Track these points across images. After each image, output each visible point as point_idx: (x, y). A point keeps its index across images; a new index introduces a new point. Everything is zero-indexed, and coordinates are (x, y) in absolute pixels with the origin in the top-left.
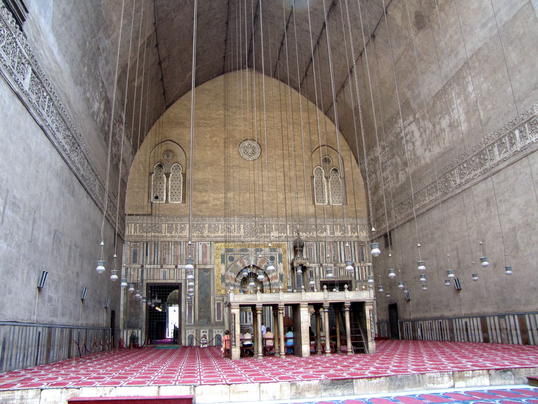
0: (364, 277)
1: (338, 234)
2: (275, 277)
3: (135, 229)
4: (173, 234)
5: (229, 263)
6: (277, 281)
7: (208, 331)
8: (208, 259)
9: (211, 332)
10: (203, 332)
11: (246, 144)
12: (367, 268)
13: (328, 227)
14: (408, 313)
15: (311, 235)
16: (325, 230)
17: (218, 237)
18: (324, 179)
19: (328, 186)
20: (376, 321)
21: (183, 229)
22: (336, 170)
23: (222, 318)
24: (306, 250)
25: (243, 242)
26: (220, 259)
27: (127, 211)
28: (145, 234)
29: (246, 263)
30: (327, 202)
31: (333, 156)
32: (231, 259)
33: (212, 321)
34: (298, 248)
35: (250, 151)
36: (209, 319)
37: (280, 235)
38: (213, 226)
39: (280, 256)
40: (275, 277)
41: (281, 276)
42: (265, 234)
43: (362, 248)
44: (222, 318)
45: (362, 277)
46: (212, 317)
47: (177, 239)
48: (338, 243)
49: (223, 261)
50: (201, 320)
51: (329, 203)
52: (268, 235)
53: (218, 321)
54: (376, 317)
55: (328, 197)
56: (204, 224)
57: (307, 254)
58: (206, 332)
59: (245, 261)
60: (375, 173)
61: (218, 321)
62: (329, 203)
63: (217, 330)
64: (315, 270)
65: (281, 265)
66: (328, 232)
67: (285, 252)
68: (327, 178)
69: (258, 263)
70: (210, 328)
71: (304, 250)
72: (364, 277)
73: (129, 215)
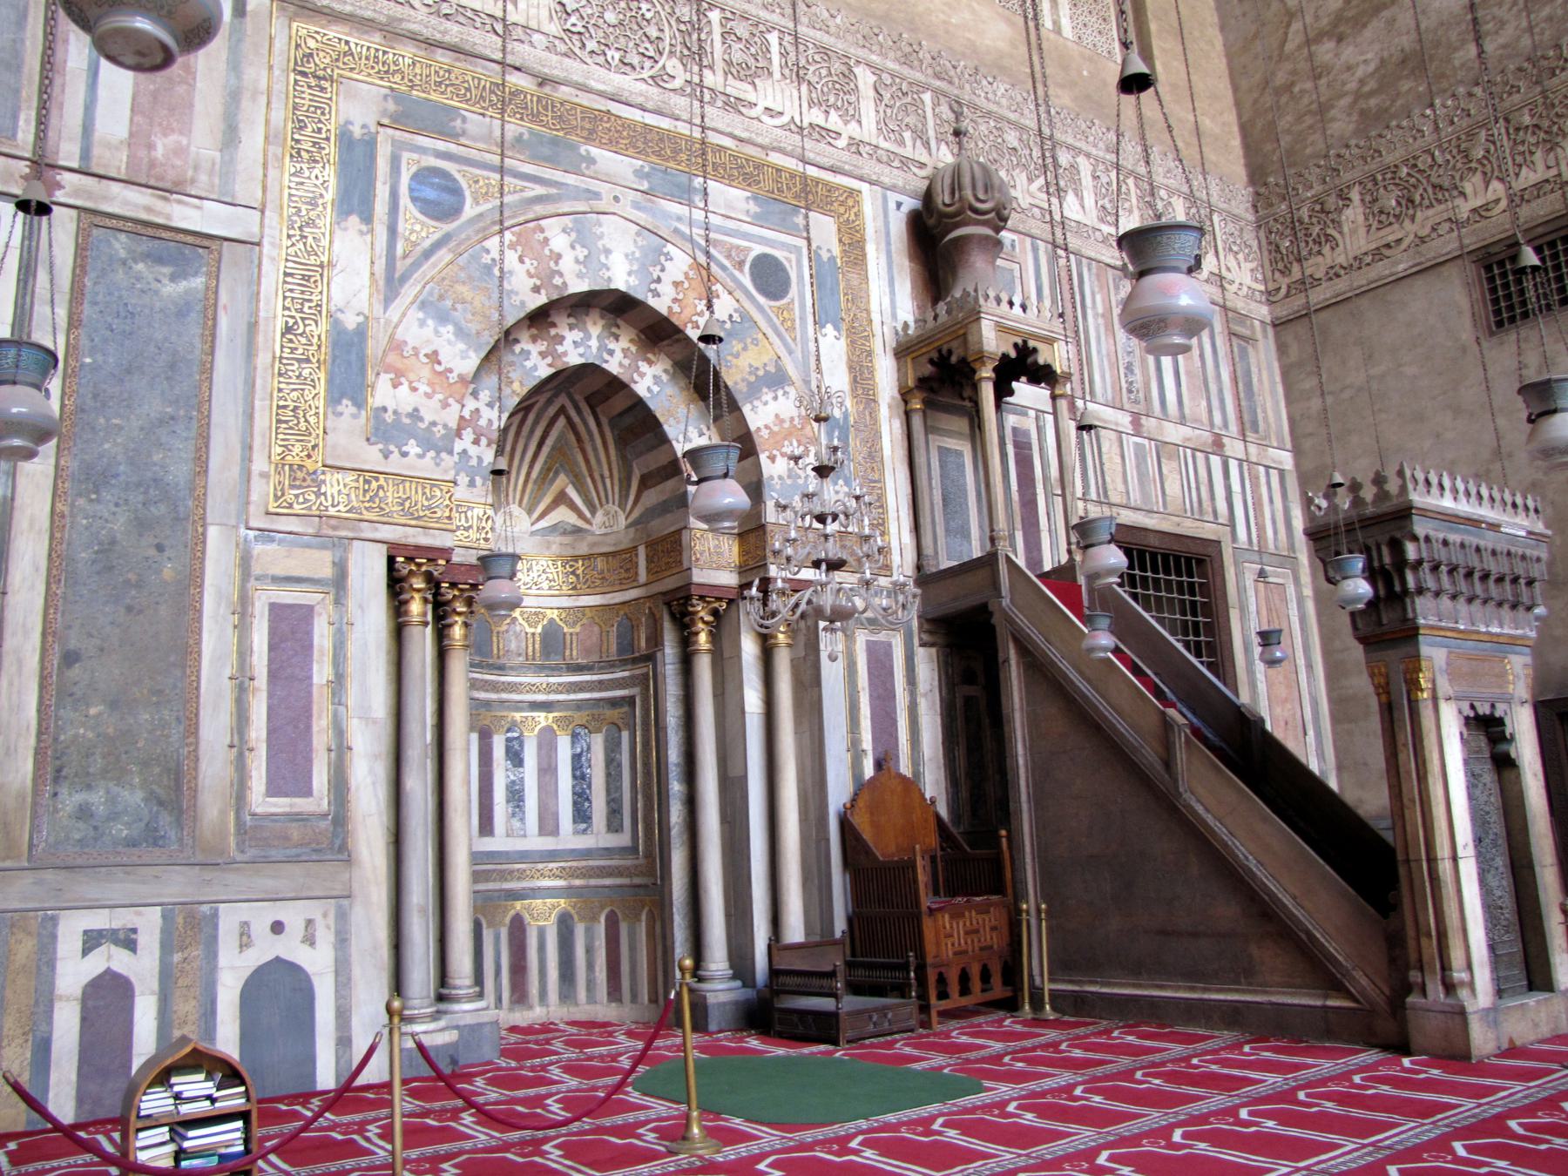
5: (416, 227)
7: (149, 924)
8: (202, 140)
9: (191, 932)
10: (92, 941)
23: (320, 778)
25: (543, 81)
26: (330, 174)
29: (567, 265)
32: (440, 197)
33: (212, 806)
34: (940, 240)
36: (174, 788)
43: (1244, 354)
44: (320, 778)
46: (213, 767)
49: (355, 199)
50: (71, 799)
53: (281, 805)
58: (128, 941)
59: (559, 242)
61: (281, 805)
63: (261, 917)
69: (667, 290)
70: (178, 885)
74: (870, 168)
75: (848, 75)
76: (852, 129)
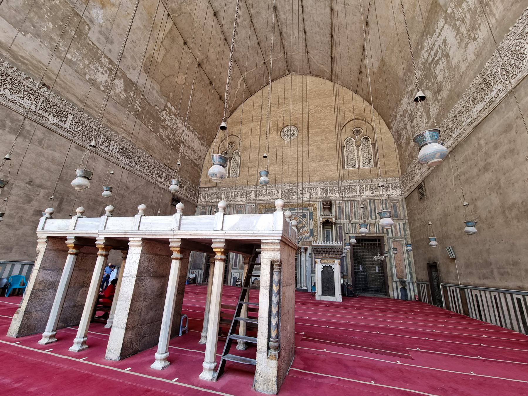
0: (399, 233)
1: (369, 193)
2: (306, 232)
3: (205, 198)
4: (229, 199)
6: (308, 235)
11: (287, 129)
12: (401, 225)
13: (358, 187)
14: (455, 276)
15: (341, 195)
16: (355, 190)
17: (261, 200)
18: (355, 147)
19: (358, 152)
20: (415, 280)
21: (236, 196)
22: (367, 139)
24: (336, 208)
27: (202, 185)
28: (211, 201)
30: (357, 166)
31: (364, 127)
34: (328, 205)
35: (289, 133)
37: (312, 196)
38: (258, 192)
39: (311, 214)
40: (306, 232)
41: (312, 231)
42: (299, 196)
43: (395, 206)
45: (396, 233)
47: (232, 203)
48: (368, 201)
51: (359, 167)
52: (301, 196)
54: (414, 275)
55: (359, 162)
56: (251, 191)
57: (336, 211)
60: (405, 128)
62: (359, 167)
64: (344, 226)
65: (311, 222)
66: (358, 192)
67: (316, 210)
68: (358, 146)
71: (334, 209)
72: (399, 233)
73: (202, 188)
74: (318, 200)
75: (316, 189)
76: (316, 196)
